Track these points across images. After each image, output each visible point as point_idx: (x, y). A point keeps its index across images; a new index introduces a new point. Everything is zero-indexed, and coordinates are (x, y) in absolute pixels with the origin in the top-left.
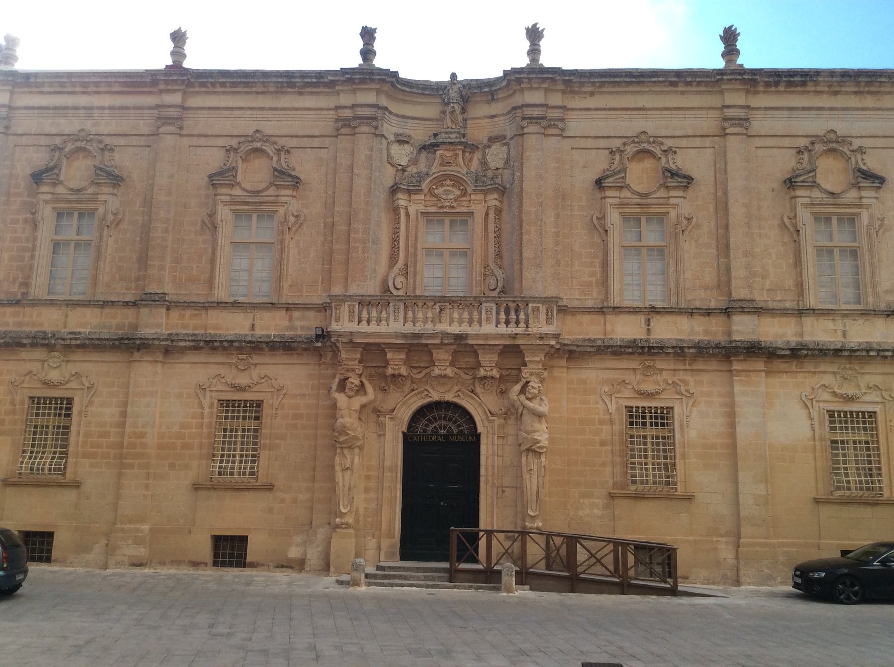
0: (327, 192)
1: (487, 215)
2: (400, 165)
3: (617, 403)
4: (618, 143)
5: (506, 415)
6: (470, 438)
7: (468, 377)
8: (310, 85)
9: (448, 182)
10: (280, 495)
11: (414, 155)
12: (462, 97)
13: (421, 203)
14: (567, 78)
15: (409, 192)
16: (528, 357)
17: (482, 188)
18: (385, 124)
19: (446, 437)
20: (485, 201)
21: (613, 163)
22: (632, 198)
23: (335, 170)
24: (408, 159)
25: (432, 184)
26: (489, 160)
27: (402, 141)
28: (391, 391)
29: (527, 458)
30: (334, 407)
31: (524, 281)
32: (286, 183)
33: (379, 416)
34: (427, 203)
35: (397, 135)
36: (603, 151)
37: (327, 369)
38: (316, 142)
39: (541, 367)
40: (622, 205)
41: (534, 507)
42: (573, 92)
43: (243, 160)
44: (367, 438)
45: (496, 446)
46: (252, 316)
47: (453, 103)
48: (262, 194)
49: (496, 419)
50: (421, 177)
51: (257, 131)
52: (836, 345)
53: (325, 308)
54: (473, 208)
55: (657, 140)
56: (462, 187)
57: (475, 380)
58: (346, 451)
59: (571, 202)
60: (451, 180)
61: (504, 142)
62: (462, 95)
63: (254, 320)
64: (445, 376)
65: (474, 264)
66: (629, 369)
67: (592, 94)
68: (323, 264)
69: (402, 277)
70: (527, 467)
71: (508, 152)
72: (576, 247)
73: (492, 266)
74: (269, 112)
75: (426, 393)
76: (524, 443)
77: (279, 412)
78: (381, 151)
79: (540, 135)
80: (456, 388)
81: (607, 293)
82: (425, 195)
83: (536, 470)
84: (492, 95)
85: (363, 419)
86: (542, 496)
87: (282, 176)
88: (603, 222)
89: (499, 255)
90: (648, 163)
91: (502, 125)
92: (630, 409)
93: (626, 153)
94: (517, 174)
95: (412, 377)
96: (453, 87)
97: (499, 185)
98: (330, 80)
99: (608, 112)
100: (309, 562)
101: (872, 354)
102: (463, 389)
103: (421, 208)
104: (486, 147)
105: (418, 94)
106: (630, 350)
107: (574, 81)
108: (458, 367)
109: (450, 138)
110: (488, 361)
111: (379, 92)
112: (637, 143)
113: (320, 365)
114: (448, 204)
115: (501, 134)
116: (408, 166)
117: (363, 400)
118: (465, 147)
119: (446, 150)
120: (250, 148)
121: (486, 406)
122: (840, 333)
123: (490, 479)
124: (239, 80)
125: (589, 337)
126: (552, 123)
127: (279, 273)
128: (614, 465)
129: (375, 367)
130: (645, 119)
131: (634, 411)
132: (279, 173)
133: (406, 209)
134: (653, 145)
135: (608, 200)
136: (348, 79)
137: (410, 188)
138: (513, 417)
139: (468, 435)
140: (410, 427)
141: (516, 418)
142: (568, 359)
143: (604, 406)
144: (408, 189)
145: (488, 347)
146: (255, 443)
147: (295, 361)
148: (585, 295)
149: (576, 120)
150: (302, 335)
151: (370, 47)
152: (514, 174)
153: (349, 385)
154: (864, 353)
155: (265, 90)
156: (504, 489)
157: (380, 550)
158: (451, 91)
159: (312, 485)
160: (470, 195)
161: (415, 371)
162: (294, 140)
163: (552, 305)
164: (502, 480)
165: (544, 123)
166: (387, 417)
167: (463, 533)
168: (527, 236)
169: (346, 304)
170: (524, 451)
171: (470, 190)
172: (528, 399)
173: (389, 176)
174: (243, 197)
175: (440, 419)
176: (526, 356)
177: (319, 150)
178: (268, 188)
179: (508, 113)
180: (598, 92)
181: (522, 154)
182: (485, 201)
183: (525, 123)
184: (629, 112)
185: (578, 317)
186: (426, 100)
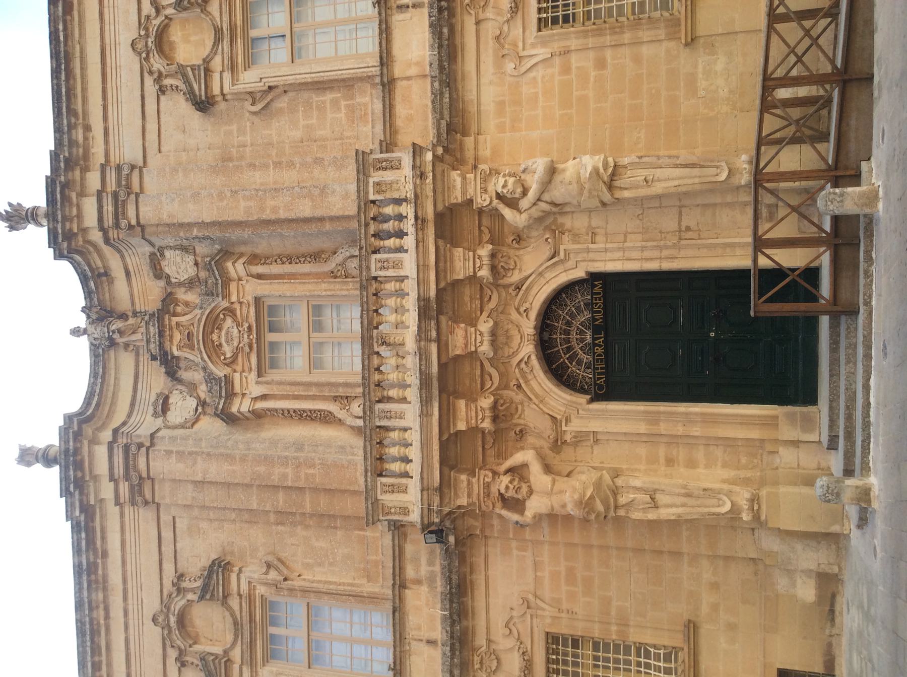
0: (234, 520)
1: (259, 277)
2: (197, 410)
3: (533, 46)
4: (149, 81)
5: (557, 231)
6: (596, 290)
7: (495, 297)
8: (90, 542)
9: (215, 337)
10: (705, 609)
11: (183, 388)
12: (100, 319)
13: (246, 378)
14: (62, 165)
15: (231, 395)
16: (456, 198)
17: (220, 286)
18: (138, 432)
19: (596, 330)
20: (240, 279)
21: (177, 87)
22: (223, 54)
23: (203, 507)
24: (188, 397)
25: (218, 361)
26: (186, 277)
27: (163, 406)
28: (522, 422)
29: (626, 189)
30: (552, 518)
31: (347, 213)
32: (221, 582)
33: (565, 442)
34: (246, 369)
35: (155, 415)
36: (162, 104)
37: (492, 526)
38: (167, 534)
39: (472, 176)
40: (233, 68)
41: (713, 171)
42: (86, 156)
43: (195, 643)
44: (602, 463)
45: (608, 245)
46: (415, 643)
47: (109, 332)
48: (239, 619)
49: (562, 248)
50: (210, 379)
51: (154, 620)
53: (398, 528)
54: (250, 298)
55: (143, 23)
56: (222, 316)
57: (498, 285)
58: (622, 500)
59: (233, 147)
60: (212, 332)
61: (158, 254)
62: (97, 319)
63: (421, 640)
64: (493, 333)
65: (329, 293)
66: (477, 32)
67: (87, 128)
68: (336, 528)
69: (352, 405)
70: (642, 187)
71: (171, 248)
72: (297, 134)
73: (331, 265)
74: (130, 601)
75: (523, 365)
76: (598, 196)
77: (565, 606)
78: (173, 439)
79: (140, 200)
80: (514, 315)
81: (361, 79)
82: (235, 371)
83: (645, 172)
84: (100, 275)
85: (569, 469)
86: (693, 159)
87: (211, 588)
88: (259, 95)
89: (316, 256)
90: (176, 34)
91: (137, 258)
92: (542, 24)
93: (162, 70)
94: (195, 232)
95: (498, 389)
96: (90, 333)
97: (213, 259)
98: (81, 512)
99: (110, 101)
100: (822, 566)
102: (516, 304)
103: (253, 376)
104: (169, 282)
105: (103, 383)
106: (445, 30)
107: (67, 154)
108: (479, 313)
109: (154, 335)
110: (464, 264)
111: (94, 441)
112: (148, 55)
113: (486, 537)
114: (246, 336)
115: (148, 261)
116: (198, 398)
117: (536, 469)
118: (168, 312)
119: (171, 341)
120: (177, 632)
121: (542, 264)
123: (665, 253)
124: (88, 644)
125: (430, 104)
126: (124, 183)
127: (351, 598)
128: (637, 43)
129: (483, 447)
130: (117, 46)
131: (545, 15)
132: (207, 593)
133: (255, 399)
134: (151, 29)
135: (226, 90)
136: (75, 488)
137: (223, 394)
138: (561, 220)
139: (593, 294)
140: (582, 391)
141: (563, 213)
142: (465, 134)
143: (540, 67)
144: (226, 398)
145: (441, 264)
146: (617, 647)
147: (483, 577)
148: (366, 114)
149: (122, 149)
150: (441, 564)
151: (40, 455)
152: (197, 237)
153: (511, 493)
155: (102, 606)
156: (683, 228)
157: (799, 441)
158: (96, 336)
159: (686, 557)
160: (232, 303)
161: (488, 384)
162: (165, 566)
163: (371, 161)
164: (668, 233)
165: (122, 196)
166: (564, 428)
167: (761, 294)
168: (281, 211)
169: (380, 497)
170: (612, 195)
171: (224, 304)
172: (525, 192)
173: (210, 425)
174: (245, 646)
175: (568, 341)
176: (455, 201)
177: (177, 530)
178: (230, 609)
179: (119, 251)
180: (84, 119)
181: (168, 225)
182: (240, 279)
183: (123, 223)
185: (399, 122)
186: (113, 372)
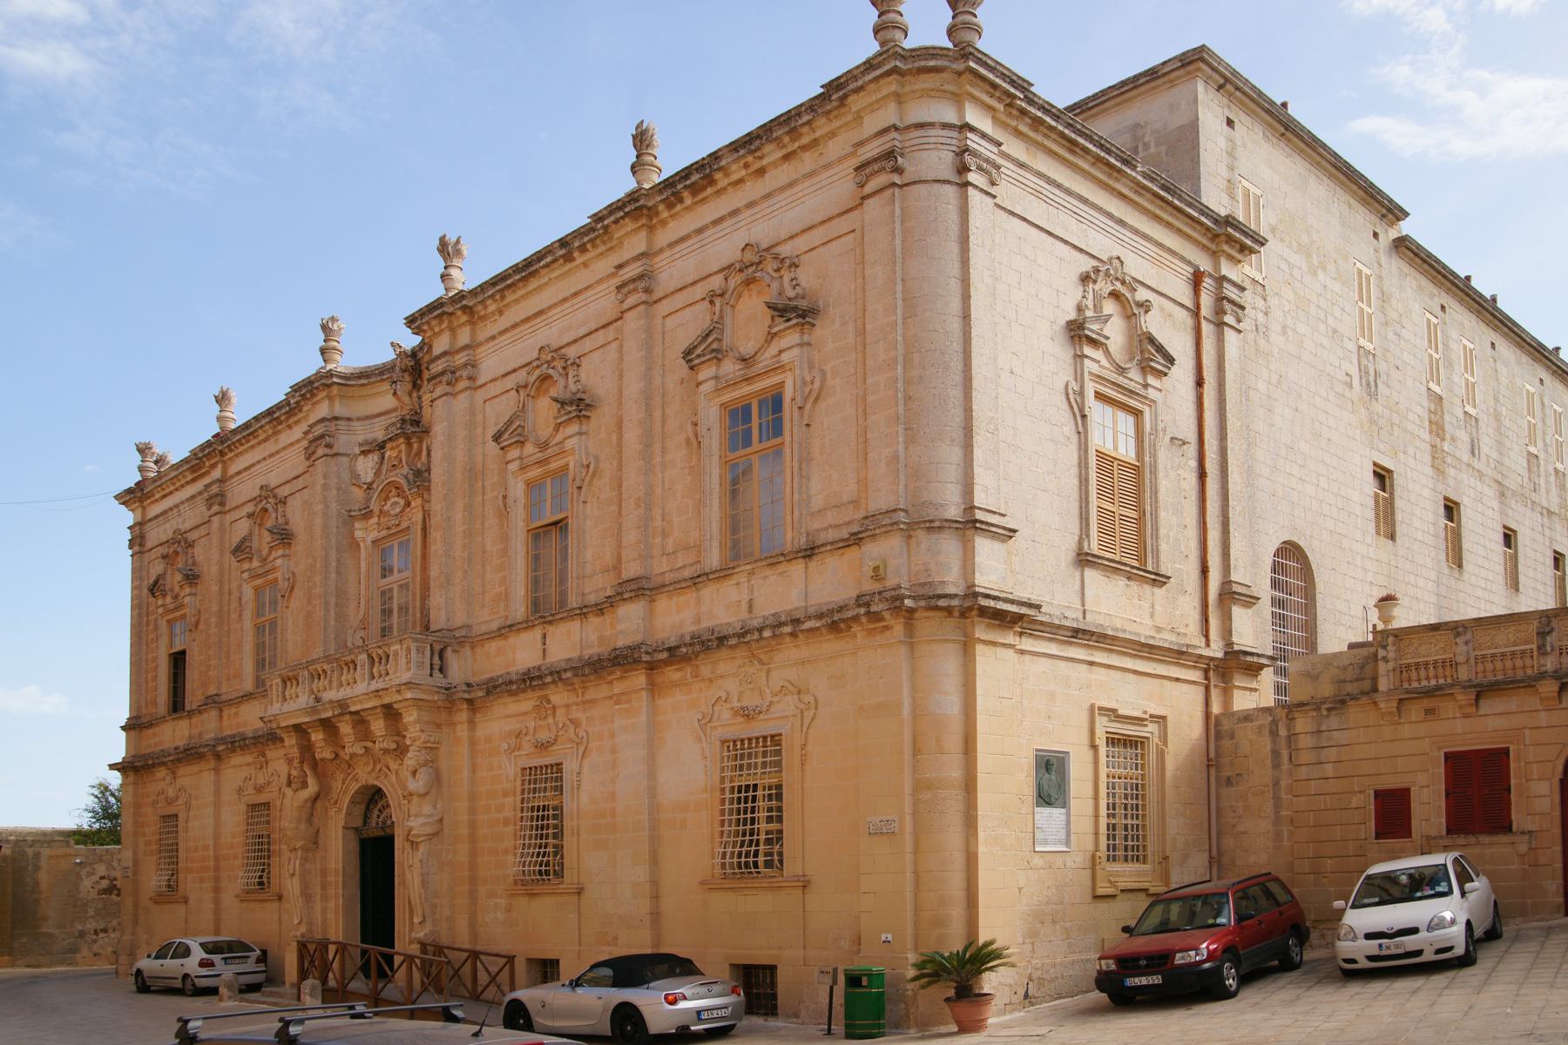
42: (482, 318)
52: (734, 628)
67: (501, 313)
101: (767, 634)
122: (744, 605)
154: (756, 636)
184: (532, 323)
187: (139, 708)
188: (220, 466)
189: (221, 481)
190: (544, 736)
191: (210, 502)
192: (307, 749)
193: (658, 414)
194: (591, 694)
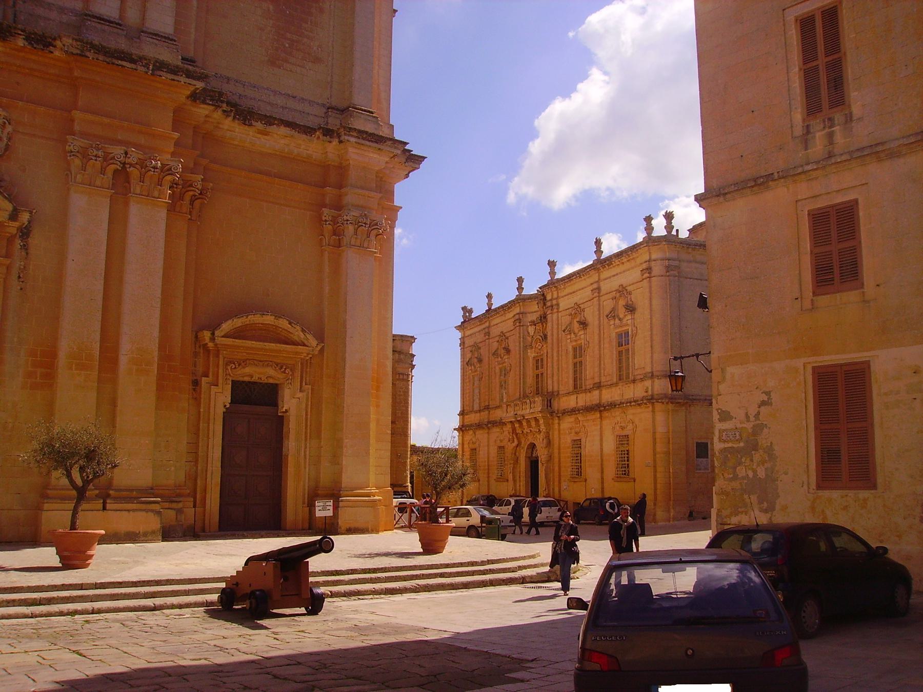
187: (463, 407)
188: (488, 322)
189: (489, 327)
190: (577, 430)
191: (485, 335)
192: (514, 430)
193: (602, 331)
194: (588, 418)
